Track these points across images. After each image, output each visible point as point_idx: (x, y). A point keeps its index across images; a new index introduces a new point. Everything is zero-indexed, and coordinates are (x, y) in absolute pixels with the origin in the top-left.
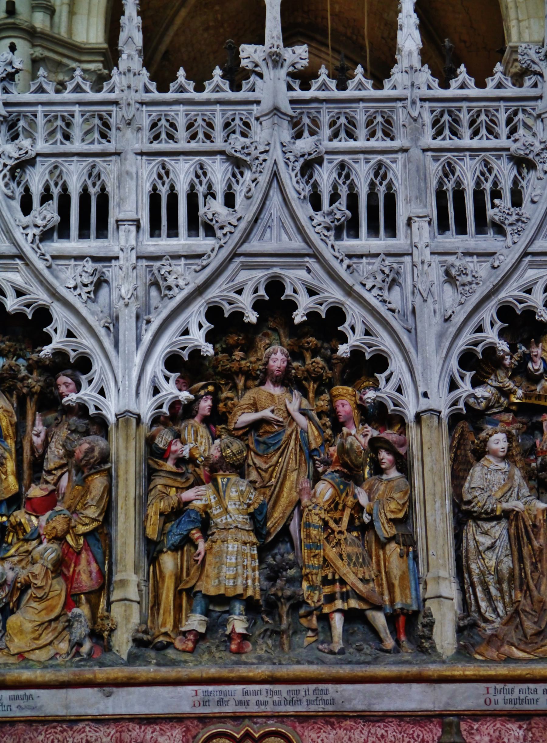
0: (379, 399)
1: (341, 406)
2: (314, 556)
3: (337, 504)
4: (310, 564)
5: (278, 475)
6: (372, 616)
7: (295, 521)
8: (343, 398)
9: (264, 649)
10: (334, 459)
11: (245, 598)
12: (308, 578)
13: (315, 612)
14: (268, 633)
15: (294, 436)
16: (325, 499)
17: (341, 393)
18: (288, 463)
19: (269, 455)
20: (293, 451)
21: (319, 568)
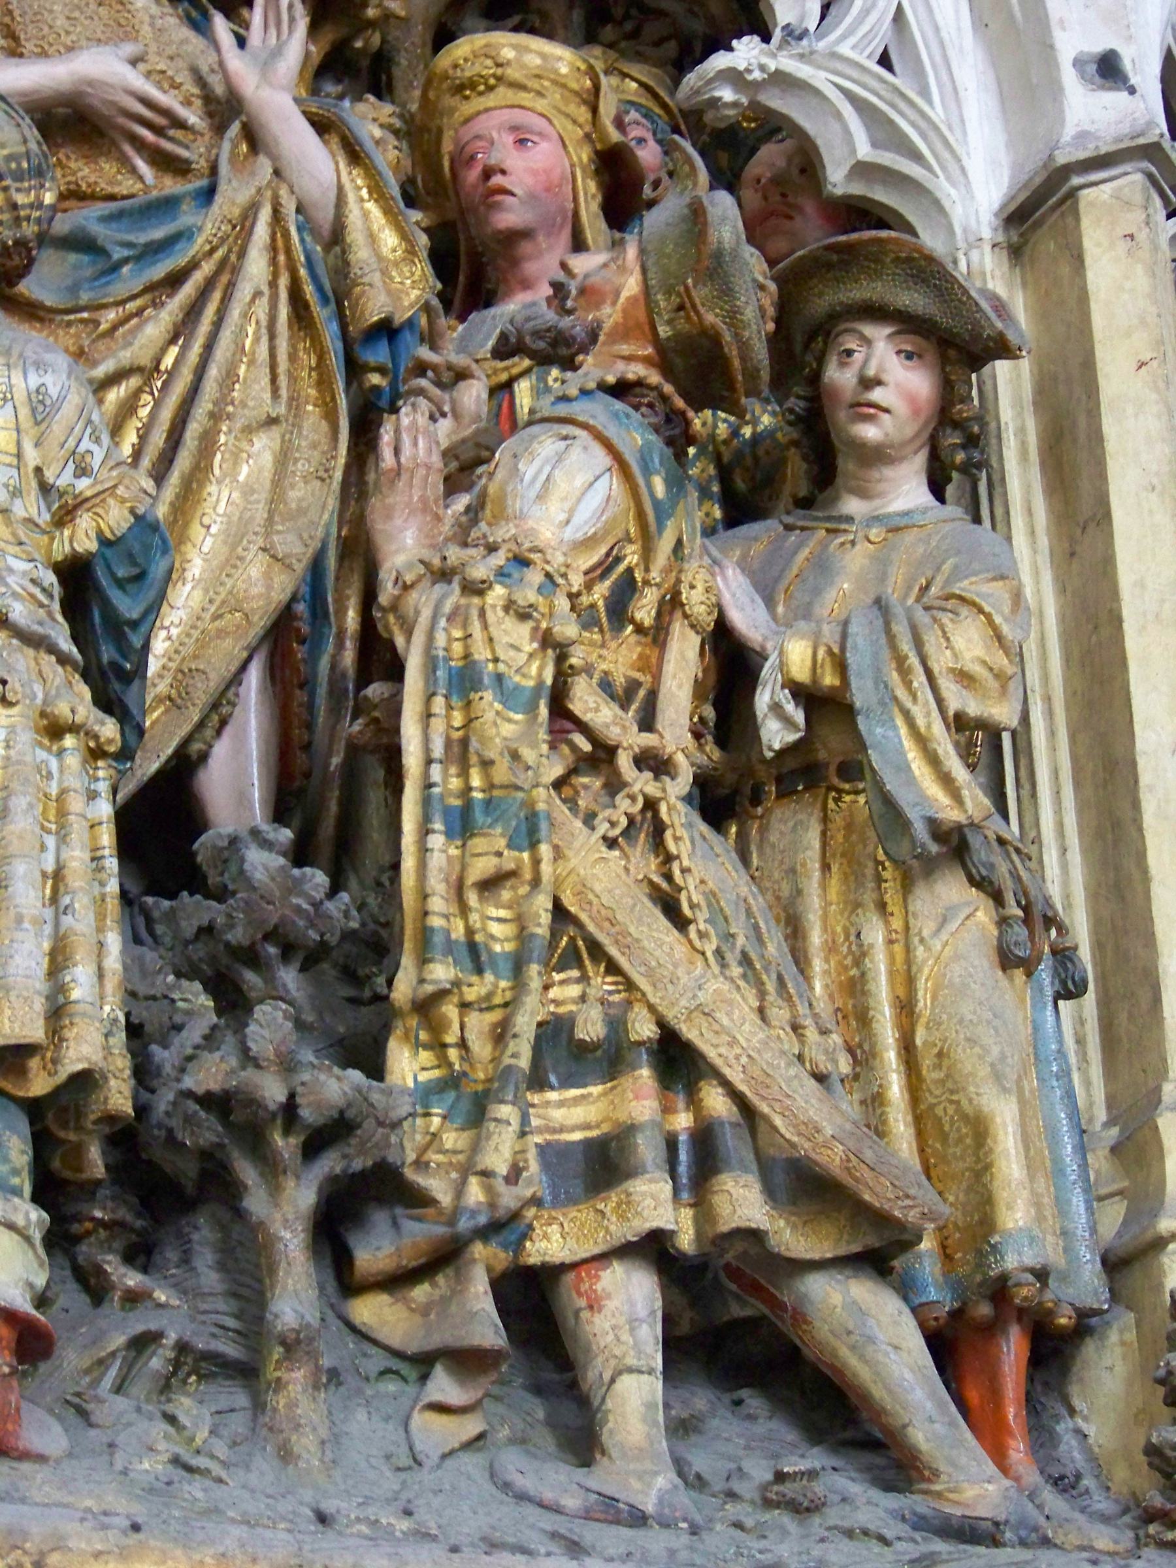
0: (775, 101)
1: (509, 139)
2: (490, 885)
3: (627, 588)
4: (458, 931)
5: (158, 439)
6: (854, 1307)
7: (241, 740)
8: (525, 98)
9: (162, 1446)
10: (610, 315)
11: (39, 1085)
12: (436, 1027)
13: (479, 1250)
14: (157, 1362)
15: (262, 231)
16: (569, 534)
17: (512, 73)
18: (230, 377)
19: (111, 316)
20: (261, 310)
21: (518, 965)
